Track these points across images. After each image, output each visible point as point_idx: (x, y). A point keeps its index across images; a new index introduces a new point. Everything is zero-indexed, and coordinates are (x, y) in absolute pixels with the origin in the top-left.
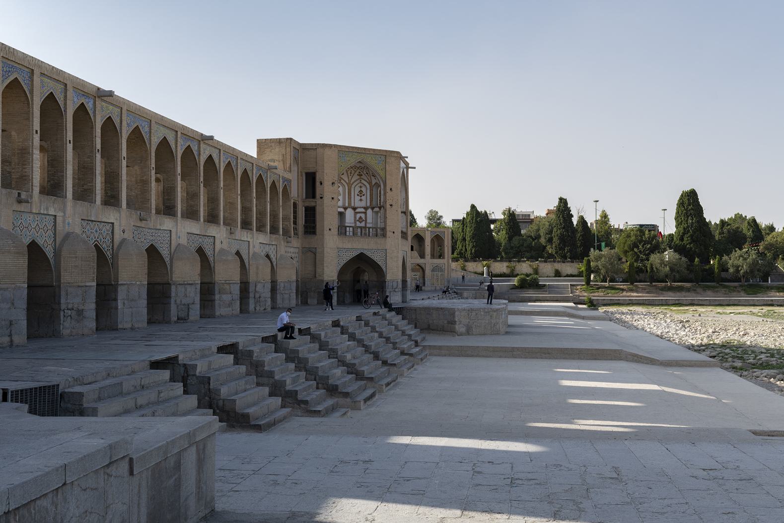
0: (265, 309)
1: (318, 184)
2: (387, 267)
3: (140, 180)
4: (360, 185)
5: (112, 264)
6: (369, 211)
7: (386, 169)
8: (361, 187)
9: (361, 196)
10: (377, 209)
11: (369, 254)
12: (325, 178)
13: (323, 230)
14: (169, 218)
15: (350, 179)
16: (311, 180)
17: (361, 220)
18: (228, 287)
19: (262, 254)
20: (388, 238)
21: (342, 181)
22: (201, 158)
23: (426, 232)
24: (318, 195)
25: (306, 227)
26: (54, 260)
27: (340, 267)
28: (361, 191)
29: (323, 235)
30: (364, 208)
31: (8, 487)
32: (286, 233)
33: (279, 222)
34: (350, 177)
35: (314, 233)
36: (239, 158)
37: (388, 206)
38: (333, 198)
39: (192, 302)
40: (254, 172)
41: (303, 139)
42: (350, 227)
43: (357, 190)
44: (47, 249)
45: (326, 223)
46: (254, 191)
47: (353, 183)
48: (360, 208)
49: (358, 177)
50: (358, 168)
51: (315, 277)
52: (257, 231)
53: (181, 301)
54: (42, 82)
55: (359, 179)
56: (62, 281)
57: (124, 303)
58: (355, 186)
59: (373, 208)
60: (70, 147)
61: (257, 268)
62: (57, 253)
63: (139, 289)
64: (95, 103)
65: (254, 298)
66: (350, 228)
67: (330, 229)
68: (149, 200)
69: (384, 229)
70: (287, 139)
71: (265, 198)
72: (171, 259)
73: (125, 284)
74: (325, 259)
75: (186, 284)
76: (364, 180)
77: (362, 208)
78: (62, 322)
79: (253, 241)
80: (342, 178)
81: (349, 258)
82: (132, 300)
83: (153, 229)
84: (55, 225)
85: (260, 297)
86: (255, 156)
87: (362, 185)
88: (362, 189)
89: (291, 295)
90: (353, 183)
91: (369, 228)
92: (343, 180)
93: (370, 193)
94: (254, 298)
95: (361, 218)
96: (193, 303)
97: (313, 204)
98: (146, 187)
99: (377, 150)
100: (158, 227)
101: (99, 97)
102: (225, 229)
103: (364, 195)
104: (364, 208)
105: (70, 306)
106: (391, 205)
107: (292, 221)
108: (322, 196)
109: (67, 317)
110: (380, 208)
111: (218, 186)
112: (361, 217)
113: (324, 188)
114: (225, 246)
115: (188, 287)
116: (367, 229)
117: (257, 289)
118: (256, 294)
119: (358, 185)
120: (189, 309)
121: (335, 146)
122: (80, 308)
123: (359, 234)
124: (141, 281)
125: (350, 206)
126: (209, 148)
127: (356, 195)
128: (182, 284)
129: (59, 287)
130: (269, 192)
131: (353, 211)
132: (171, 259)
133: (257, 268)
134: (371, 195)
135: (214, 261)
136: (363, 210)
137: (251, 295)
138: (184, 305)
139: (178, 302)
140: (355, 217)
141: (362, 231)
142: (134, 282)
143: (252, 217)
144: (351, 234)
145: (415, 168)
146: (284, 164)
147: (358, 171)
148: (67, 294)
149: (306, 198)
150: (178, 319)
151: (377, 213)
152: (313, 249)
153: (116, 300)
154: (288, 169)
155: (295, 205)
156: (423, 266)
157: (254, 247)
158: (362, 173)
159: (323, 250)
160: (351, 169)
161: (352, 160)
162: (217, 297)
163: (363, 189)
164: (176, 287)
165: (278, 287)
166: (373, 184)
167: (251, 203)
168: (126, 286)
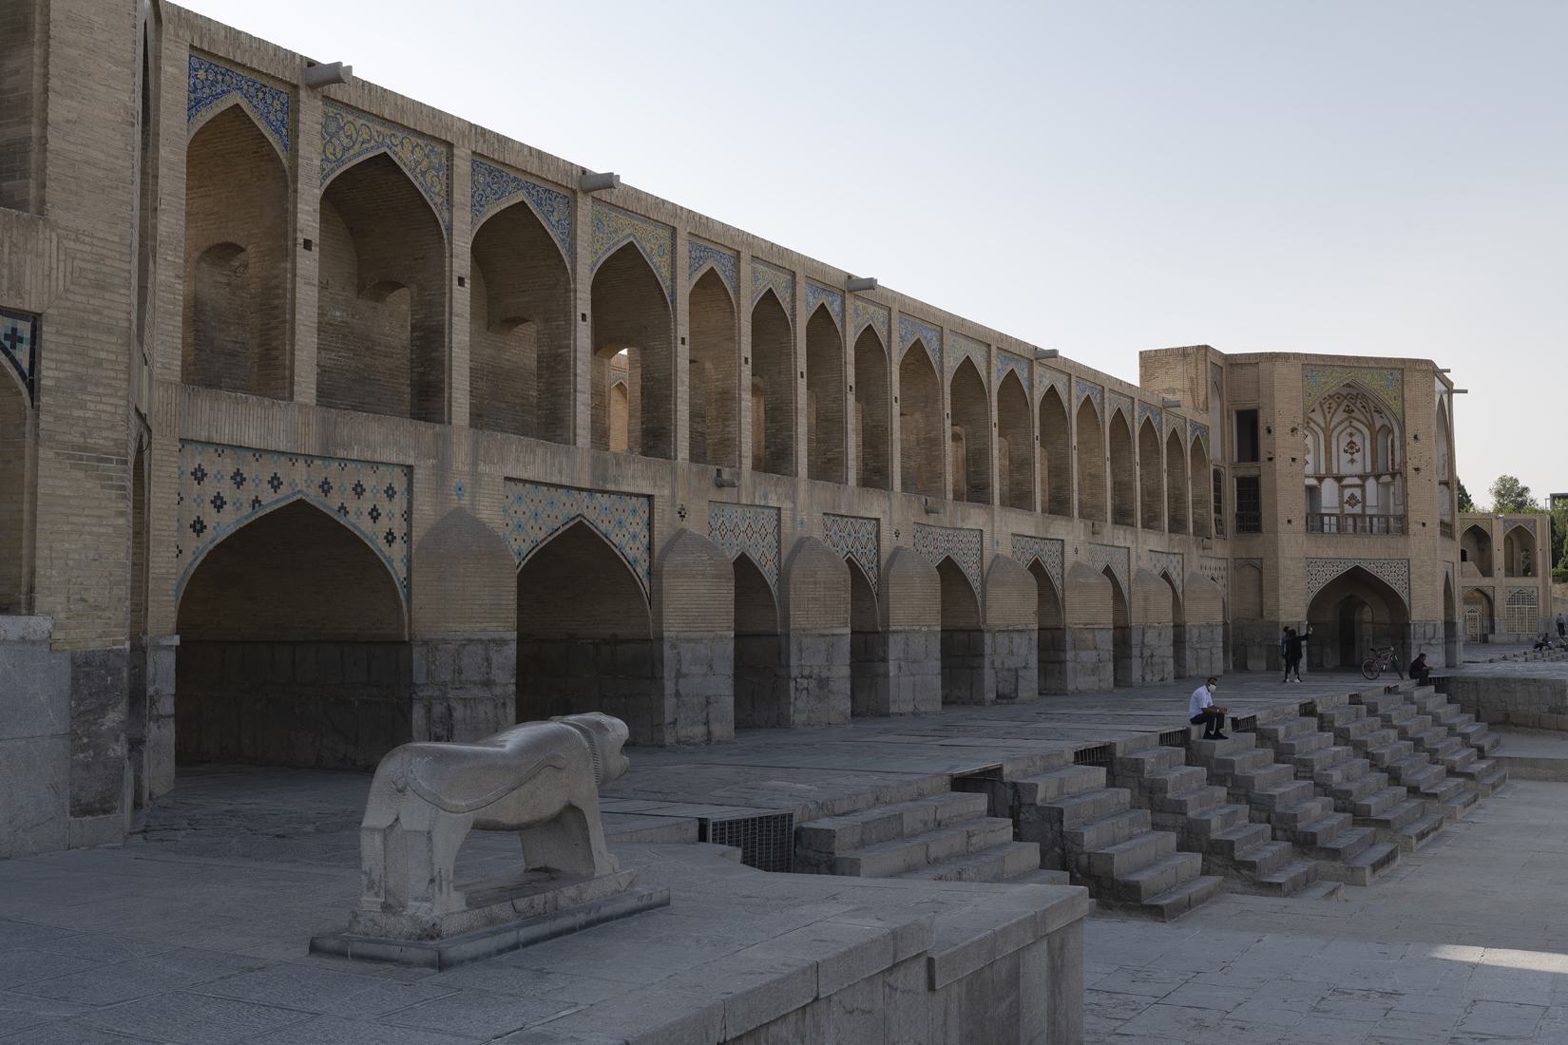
0: (1162, 680)
1: (1262, 432)
2: (1412, 596)
3: (924, 439)
4: (1349, 430)
5: (877, 595)
6: (1371, 484)
7: (1403, 395)
8: (1351, 435)
10: (1386, 479)
11: (1371, 569)
12: (1278, 420)
13: (1275, 524)
14: (978, 507)
15: (1328, 420)
16: (1248, 426)
18: (1090, 636)
19: (1156, 572)
20: (1412, 537)
21: (1312, 425)
22: (1036, 392)
23: (1494, 522)
24: (1263, 455)
25: (1240, 517)
26: (778, 588)
27: (1312, 596)
28: (1352, 442)
29: (1276, 533)
30: (1360, 477)
31: (724, 997)
32: (1200, 529)
33: (1186, 509)
34: (1329, 416)
35: (1257, 528)
36: (1106, 390)
37: (1410, 471)
38: (1293, 460)
39: (1024, 664)
40: (1136, 414)
41: (1228, 347)
42: (1332, 515)
43: (1344, 440)
44: (766, 569)
45: (1280, 508)
46: (1137, 450)
47: (1335, 427)
48: (1351, 476)
49: (1346, 415)
50: (1345, 398)
51: (1262, 616)
52: (1143, 527)
53: (1003, 663)
54: (754, 271)
55: (1346, 419)
56: (792, 626)
57: (900, 667)
58: (1340, 434)
59: (1377, 477)
60: (802, 384)
61: (1146, 599)
62: (783, 576)
63: (926, 641)
64: (843, 302)
65: (1141, 656)
66: (1332, 518)
67: (1289, 521)
68: (941, 475)
69: (1403, 519)
70: (1199, 347)
71: (1159, 463)
72: (984, 584)
73: (901, 632)
74: (1281, 580)
75: (1011, 631)
76: (1358, 420)
77: (1356, 476)
78: (792, 700)
79: (1137, 547)
80: (1311, 419)
81: (1330, 578)
82: (915, 661)
83: (949, 528)
84: (779, 526)
85: (1152, 656)
86: (1137, 383)
87: (1354, 431)
88: (1354, 439)
89: (1214, 651)
90: (1335, 427)
91: (1371, 517)
92: (1315, 422)
93: (1371, 445)
94: (1141, 656)
95: (1352, 496)
96: (1025, 668)
97: (1253, 472)
98: (935, 451)
99: (1384, 359)
100: (959, 525)
101: (850, 291)
102: (1083, 525)
103: (1358, 451)
104: (1360, 477)
105: (806, 672)
106: (1417, 469)
107: (1212, 507)
108: (1271, 456)
109: (802, 691)
110: (1393, 476)
111: (1068, 444)
112: (1352, 495)
114: (1083, 558)
115: (1016, 638)
116: (1368, 519)
117: (1146, 640)
118: (1145, 648)
119: (1345, 432)
120: (1017, 679)
121: (1296, 356)
122: (824, 675)
123: (1350, 529)
124: (929, 626)
125: (1329, 474)
126: (1049, 373)
127: (1342, 450)
128: (1004, 631)
129: (788, 635)
130: (1165, 451)
131: (1336, 485)
132: (984, 584)
133: (1146, 599)
134: (1374, 451)
135: (1063, 586)
136: (1357, 481)
137: (1136, 652)
138: (1009, 670)
139: (998, 664)
140: (1341, 496)
141: (1356, 524)
142: (917, 628)
143: (1133, 500)
144: (1334, 529)
145: (1466, 392)
146: (1193, 396)
147: (1346, 402)
148: (801, 650)
149: (1239, 461)
150: (998, 696)
151: (1387, 485)
152: (1258, 562)
153: (885, 660)
154: (1201, 406)
155: (1217, 475)
156: (1490, 592)
157: (1139, 558)
158: (1354, 408)
159: (1277, 562)
160: (1331, 401)
161: (1333, 383)
162: (1070, 655)
163: (1357, 439)
164: (994, 637)
165: (1187, 636)
166: (1377, 429)
167: (1131, 475)
168: (903, 635)
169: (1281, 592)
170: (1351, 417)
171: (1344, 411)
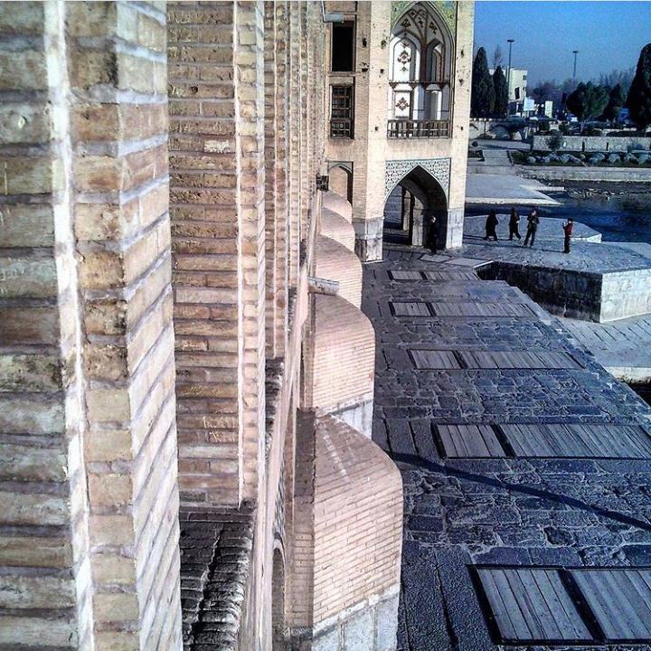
1: (359, 44)
9: (404, 63)
11: (427, 168)
17: (403, 105)
20: (454, 139)
24: (358, 67)
28: (404, 52)
29: (366, 139)
30: (411, 84)
37: (457, 82)
48: (403, 83)
49: (402, 28)
67: (376, 129)
97: (349, 81)
106: (461, 81)
112: (403, 99)
113: (369, 52)
152: (349, 165)
169: (368, 193)
170: (405, 30)
171: (402, 25)
